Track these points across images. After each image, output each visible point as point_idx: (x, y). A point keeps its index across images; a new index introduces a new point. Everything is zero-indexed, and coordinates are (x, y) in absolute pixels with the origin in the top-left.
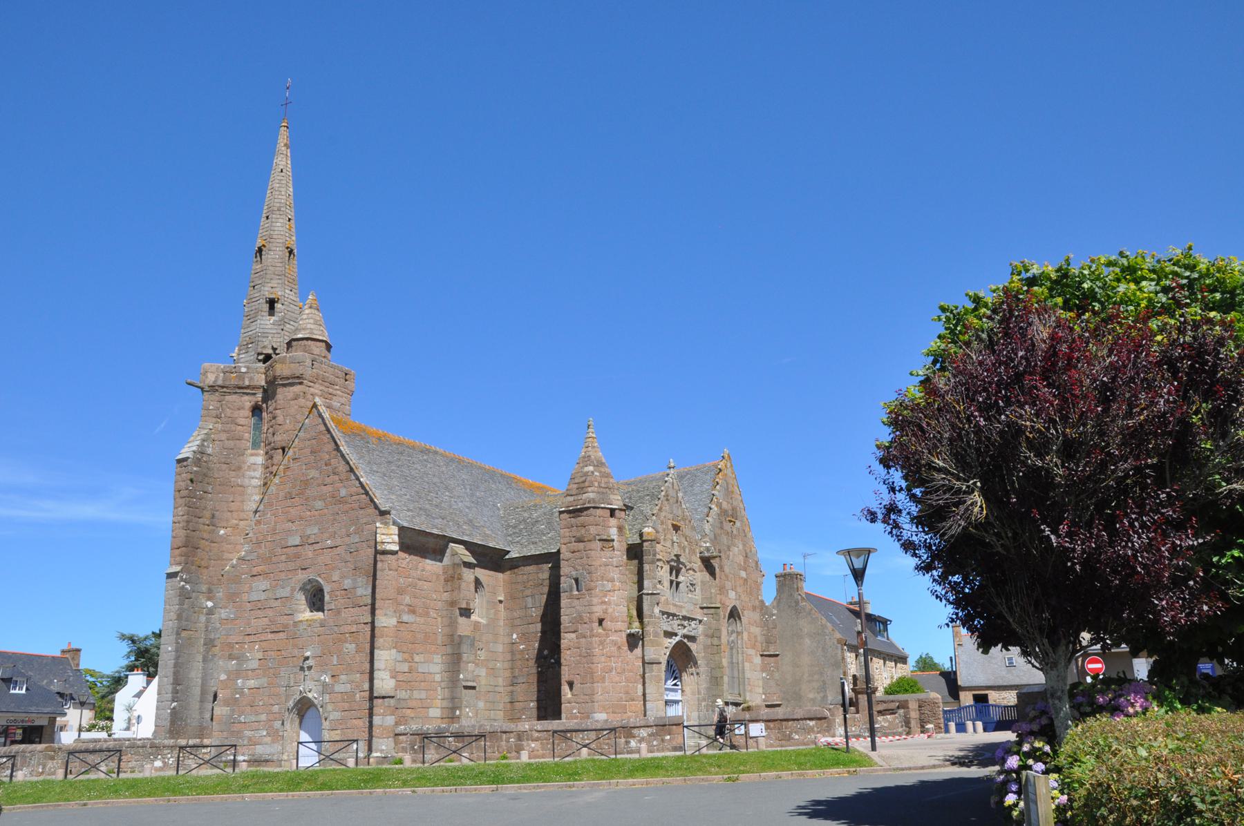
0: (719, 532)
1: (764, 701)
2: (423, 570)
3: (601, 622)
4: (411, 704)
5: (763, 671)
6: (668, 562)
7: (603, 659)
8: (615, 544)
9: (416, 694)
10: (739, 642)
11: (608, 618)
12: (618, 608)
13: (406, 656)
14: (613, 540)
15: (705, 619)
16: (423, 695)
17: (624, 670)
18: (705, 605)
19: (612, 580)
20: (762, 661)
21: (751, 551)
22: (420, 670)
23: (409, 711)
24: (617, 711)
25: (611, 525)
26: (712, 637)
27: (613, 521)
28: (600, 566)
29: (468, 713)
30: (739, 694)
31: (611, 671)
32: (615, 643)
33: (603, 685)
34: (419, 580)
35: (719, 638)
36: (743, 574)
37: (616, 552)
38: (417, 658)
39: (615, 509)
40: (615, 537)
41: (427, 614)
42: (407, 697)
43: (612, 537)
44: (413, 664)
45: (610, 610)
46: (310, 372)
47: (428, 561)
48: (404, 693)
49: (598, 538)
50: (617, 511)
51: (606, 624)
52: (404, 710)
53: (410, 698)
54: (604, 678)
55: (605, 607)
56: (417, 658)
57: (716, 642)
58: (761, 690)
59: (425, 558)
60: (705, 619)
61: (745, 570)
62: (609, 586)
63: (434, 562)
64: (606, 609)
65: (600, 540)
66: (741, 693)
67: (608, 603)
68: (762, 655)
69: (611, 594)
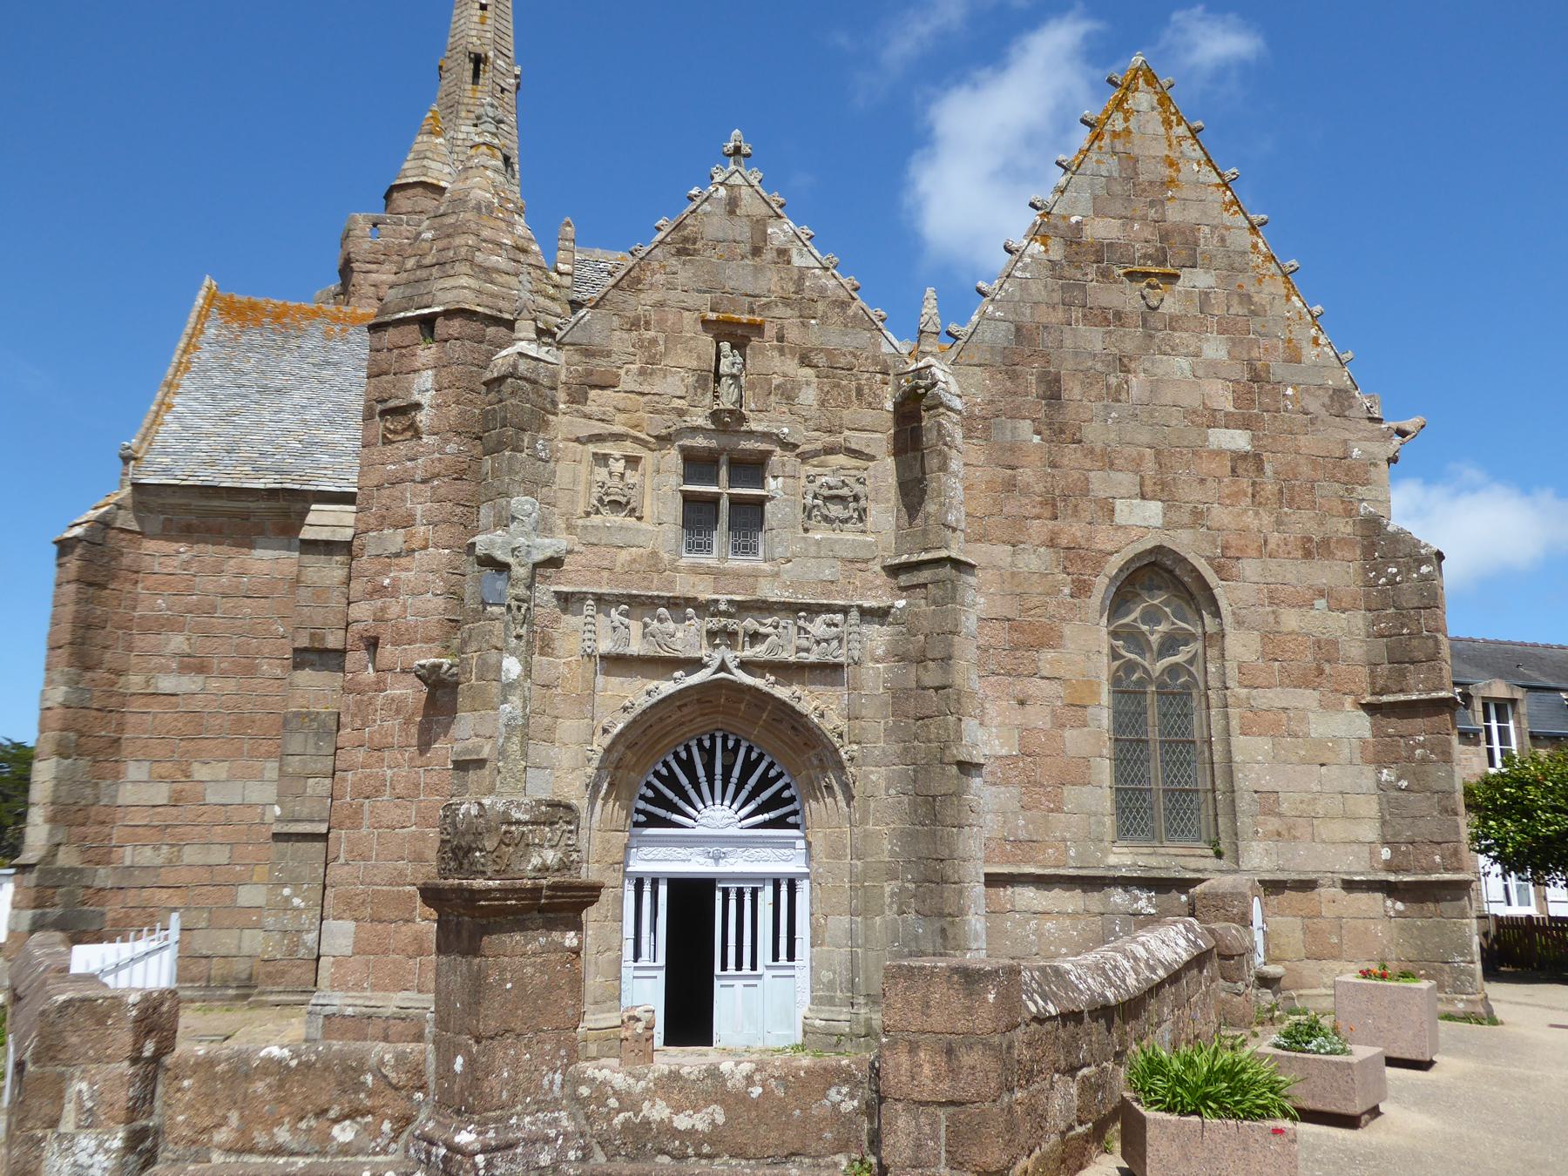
0: (1059, 315)
1: (1389, 867)
2: (239, 575)
3: (372, 644)
4: (169, 877)
5: (1380, 764)
6: (664, 440)
7: (360, 755)
8: (422, 418)
9: (191, 855)
10: (1212, 668)
11: (386, 635)
12: (418, 602)
13: (165, 768)
14: (417, 406)
15: (901, 603)
16: (220, 855)
17: (417, 785)
18: (904, 558)
19: (407, 522)
20: (1377, 732)
21: (1294, 357)
22: (210, 799)
23: (164, 894)
24: (386, 913)
25: (418, 364)
26: (921, 660)
27: (426, 353)
28: (379, 487)
29: (288, 899)
30: (1214, 844)
31: (378, 791)
32: (397, 706)
33: (353, 834)
34: (225, 596)
35: (946, 659)
36: (1240, 440)
37: (425, 439)
38: (200, 772)
39: (435, 316)
40: (425, 399)
41: (250, 671)
42: (159, 861)
43: (417, 397)
44: (187, 786)
45: (394, 610)
46: (366, 246)
47: (258, 553)
48: (148, 851)
49: (379, 407)
50: (439, 321)
51: (387, 652)
52: (146, 893)
53: (170, 863)
54: (358, 811)
55: (379, 603)
56: (200, 772)
57: (932, 676)
58: (1370, 832)
59: (252, 546)
60: (901, 603)
61: (1246, 424)
62: (395, 539)
63: (277, 553)
64: (383, 609)
65: (383, 413)
66: (1222, 847)
67: (392, 591)
68: (1371, 709)
69: (403, 561)
